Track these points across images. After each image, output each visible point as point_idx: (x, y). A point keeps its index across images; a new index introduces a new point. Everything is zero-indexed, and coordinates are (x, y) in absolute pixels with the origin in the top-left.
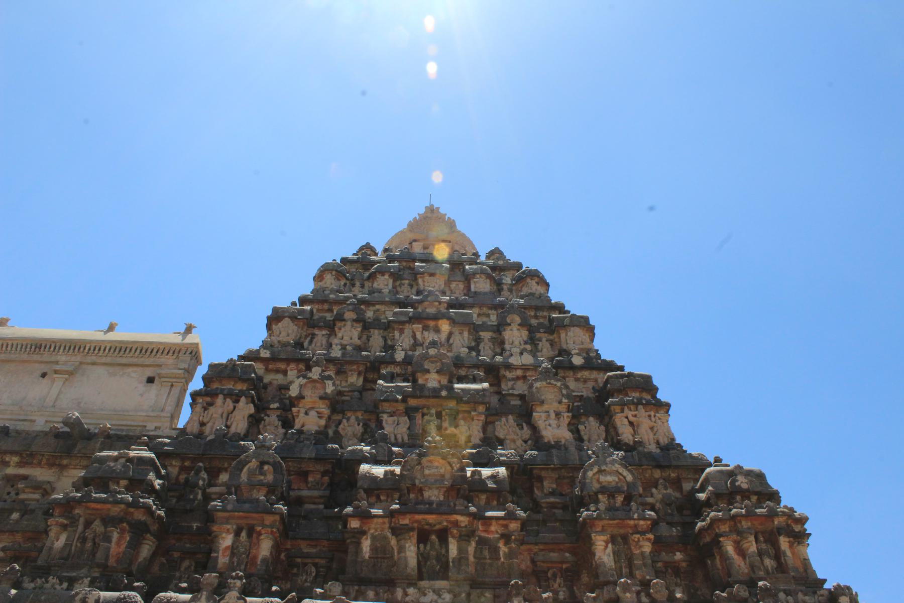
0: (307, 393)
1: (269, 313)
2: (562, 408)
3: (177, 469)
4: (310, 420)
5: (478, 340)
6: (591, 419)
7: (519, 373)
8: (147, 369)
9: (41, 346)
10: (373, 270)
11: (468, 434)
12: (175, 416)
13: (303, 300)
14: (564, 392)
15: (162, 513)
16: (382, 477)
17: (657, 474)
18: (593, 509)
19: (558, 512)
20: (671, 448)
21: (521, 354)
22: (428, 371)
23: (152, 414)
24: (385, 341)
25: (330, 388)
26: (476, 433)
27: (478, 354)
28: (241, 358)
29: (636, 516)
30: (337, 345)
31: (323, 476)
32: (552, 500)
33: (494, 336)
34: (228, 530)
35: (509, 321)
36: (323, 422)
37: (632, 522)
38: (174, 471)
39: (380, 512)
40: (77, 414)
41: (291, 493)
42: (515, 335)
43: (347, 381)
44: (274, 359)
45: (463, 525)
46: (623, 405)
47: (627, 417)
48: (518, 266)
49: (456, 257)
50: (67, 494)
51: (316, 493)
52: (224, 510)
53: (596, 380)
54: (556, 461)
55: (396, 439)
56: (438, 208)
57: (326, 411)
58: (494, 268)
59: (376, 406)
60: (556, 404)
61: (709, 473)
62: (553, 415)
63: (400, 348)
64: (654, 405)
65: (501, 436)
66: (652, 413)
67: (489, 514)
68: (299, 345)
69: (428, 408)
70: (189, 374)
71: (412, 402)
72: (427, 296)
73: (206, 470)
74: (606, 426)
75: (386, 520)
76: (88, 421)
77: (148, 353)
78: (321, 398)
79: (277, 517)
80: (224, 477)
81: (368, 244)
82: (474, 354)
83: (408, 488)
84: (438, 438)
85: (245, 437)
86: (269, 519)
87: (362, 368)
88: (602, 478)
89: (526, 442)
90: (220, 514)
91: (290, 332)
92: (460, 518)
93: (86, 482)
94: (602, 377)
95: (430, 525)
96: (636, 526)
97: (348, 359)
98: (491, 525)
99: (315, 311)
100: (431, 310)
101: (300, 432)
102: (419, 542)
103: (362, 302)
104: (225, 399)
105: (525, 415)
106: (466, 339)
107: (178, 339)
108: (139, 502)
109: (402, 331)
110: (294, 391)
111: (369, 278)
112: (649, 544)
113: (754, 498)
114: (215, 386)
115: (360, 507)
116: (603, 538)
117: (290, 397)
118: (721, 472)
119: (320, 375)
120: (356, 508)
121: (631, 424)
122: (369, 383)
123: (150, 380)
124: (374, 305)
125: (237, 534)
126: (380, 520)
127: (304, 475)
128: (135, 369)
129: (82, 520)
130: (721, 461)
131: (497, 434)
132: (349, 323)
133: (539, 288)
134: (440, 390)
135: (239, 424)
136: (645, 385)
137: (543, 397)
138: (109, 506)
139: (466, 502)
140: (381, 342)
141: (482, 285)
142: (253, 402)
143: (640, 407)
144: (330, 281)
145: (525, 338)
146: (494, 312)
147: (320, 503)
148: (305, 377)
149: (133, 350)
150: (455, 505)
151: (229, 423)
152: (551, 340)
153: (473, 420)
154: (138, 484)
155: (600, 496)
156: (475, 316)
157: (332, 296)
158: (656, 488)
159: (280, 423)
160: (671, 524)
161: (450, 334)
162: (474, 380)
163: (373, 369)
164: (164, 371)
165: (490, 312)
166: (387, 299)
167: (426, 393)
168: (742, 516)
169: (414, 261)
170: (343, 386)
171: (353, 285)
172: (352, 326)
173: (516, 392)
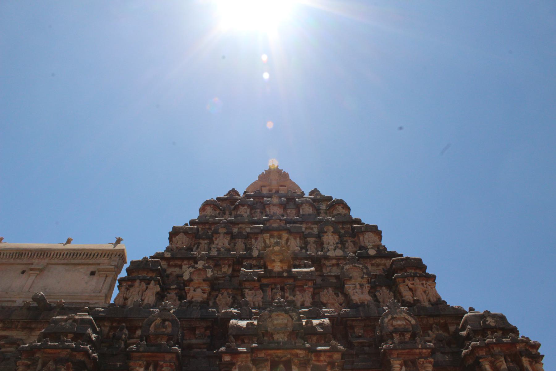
0: (195, 278)
1: (171, 230)
2: (364, 282)
3: (108, 328)
4: (197, 294)
5: (306, 243)
6: (384, 288)
7: (334, 262)
8: (90, 266)
9: (22, 253)
10: (237, 203)
11: (302, 300)
12: (108, 295)
13: (192, 222)
14: (365, 271)
15: (96, 355)
16: (245, 327)
17: (431, 321)
18: (390, 343)
19: (366, 349)
20: (439, 303)
21: (335, 250)
22: (274, 261)
23: (92, 295)
24: (246, 246)
25: (210, 273)
26: (307, 299)
27: (307, 250)
28: (151, 257)
29: (420, 346)
30: (214, 248)
31: (206, 330)
32: (361, 340)
33: (316, 240)
34: (140, 365)
35: (325, 230)
36: (205, 296)
37: (417, 351)
38: (106, 330)
39: (244, 349)
40: (42, 293)
41: (185, 342)
42: (330, 239)
43: (221, 271)
44: (172, 258)
45: (301, 356)
46: (404, 278)
47: (407, 285)
48: (330, 198)
49: (289, 194)
50: (31, 343)
51: (200, 341)
52: (137, 351)
53: (385, 265)
54: (362, 315)
55: (254, 305)
57: (206, 288)
58: (314, 200)
59: (240, 284)
60: (360, 279)
61: (467, 317)
62: (358, 286)
63: (255, 249)
64: (425, 277)
65: (325, 301)
66: (424, 282)
67: (319, 348)
68: (190, 249)
69: (275, 285)
70: (118, 269)
71: (265, 281)
72: (272, 216)
73: (127, 328)
74: (394, 293)
75: (249, 355)
76: (51, 300)
77: (92, 256)
78: (204, 280)
79: (174, 356)
80: (139, 333)
81: (233, 189)
82: (304, 251)
83: (262, 333)
84: (282, 300)
85: (154, 307)
86: (168, 357)
87: (230, 262)
88: (395, 323)
89: (341, 304)
90: (135, 354)
91: (184, 241)
92: (299, 352)
93: (45, 335)
94: (388, 262)
95: (279, 357)
96: (420, 353)
97: (222, 256)
98: (320, 356)
99: (200, 229)
100: (275, 225)
101: (190, 302)
103: (231, 222)
104: (141, 282)
105: (339, 286)
106: (298, 243)
107: (111, 247)
109: (256, 239)
110: (186, 277)
111: (234, 209)
112: (431, 365)
113: (500, 333)
114: (134, 275)
115: (230, 347)
116: (398, 362)
117: (184, 280)
118: (475, 316)
119: (203, 266)
120: (228, 347)
121: (411, 289)
122: (236, 271)
123: (93, 273)
124: (238, 224)
126: (245, 355)
127: (193, 330)
128: (83, 266)
129: (40, 361)
130: (474, 310)
131: (321, 300)
132: (222, 235)
133: (344, 210)
134: (283, 272)
135: (150, 297)
136: (417, 265)
137: (351, 275)
138: (60, 351)
139: (302, 341)
140: (243, 246)
141: (307, 210)
142: (159, 284)
143: (416, 278)
144: (209, 211)
145: (337, 241)
147: (204, 348)
148: (193, 267)
149: (82, 255)
150: (295, 343)
151: (143, 298)
152: (354, 242)
153: (305, 291)
154: (80, 336)
155: (394, 335)
156: (304, 229)
157: (211, 220)
158: (432, 331)
159: (177, 298)
160: (444, 353)
161: (287, 240)
162: (305, 267)
163: (238, 262)
164: (102, 267)
165: (313, 226)
166: (246, 220)
167: (274, 275)
168: (494, 344)
169: (264, 197)
170: (219, 274)
171: (225, 214)
172: (224, 237)
173: (333, 274)
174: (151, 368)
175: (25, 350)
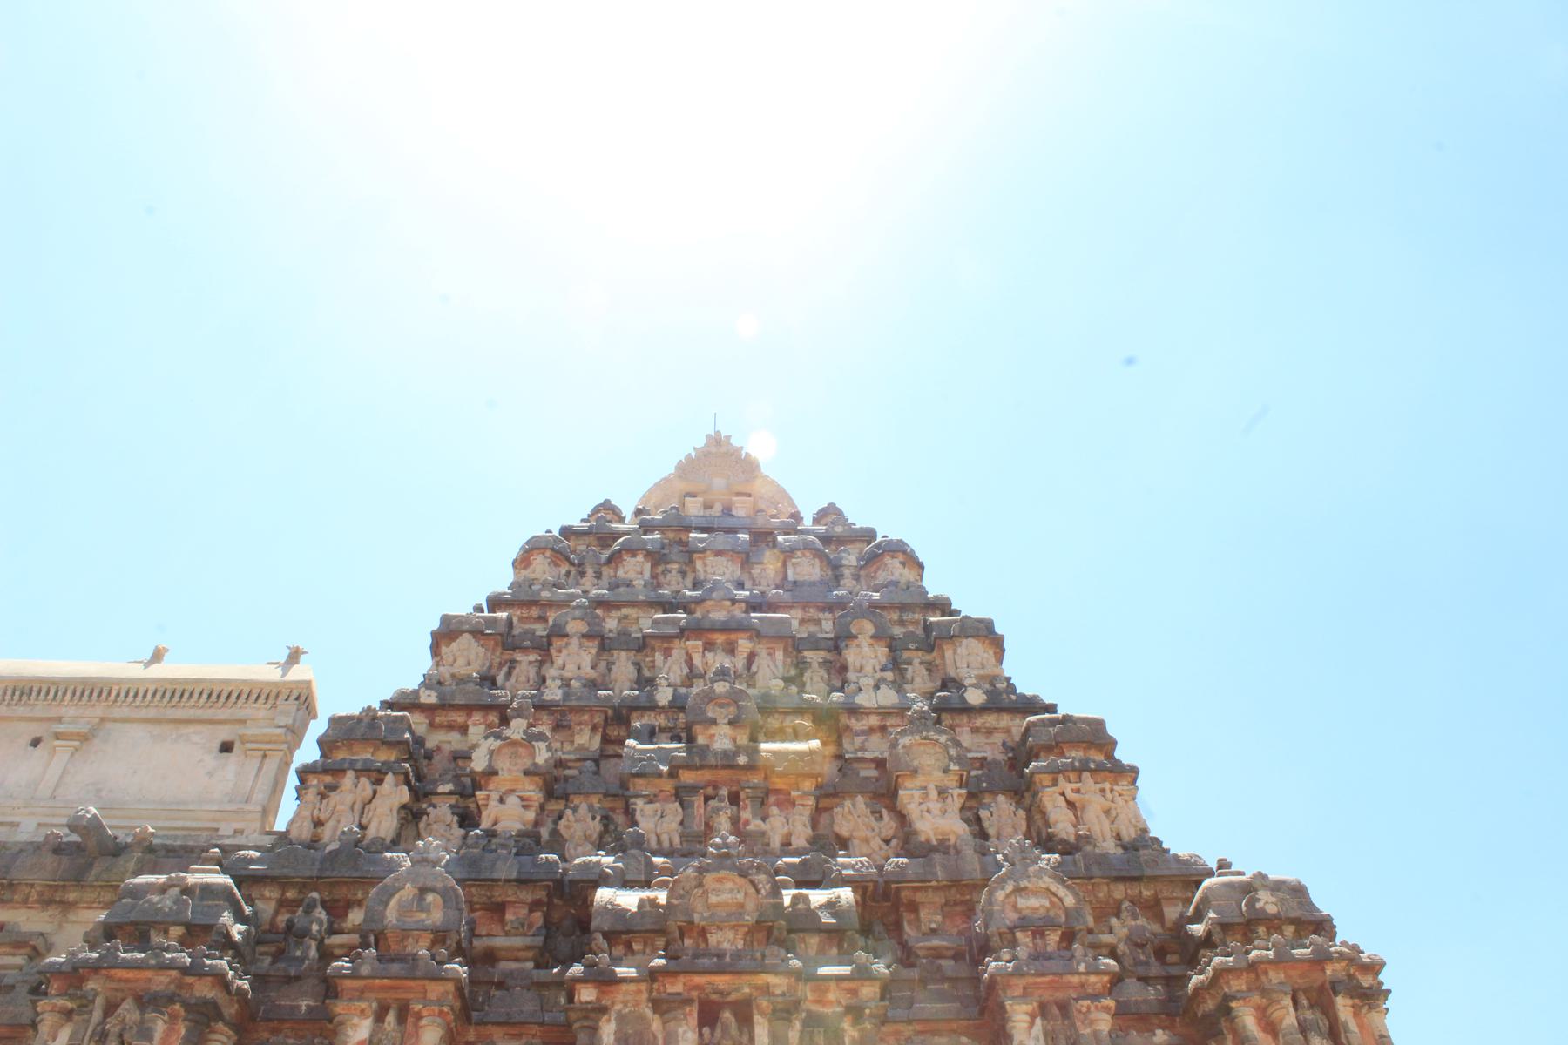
0: (503, 764)
1: (436, 625)
2: (951, 781)
3: (273, 904)
4: (507, 813)
5: (802, 665)
6: (1001, 798)
7: (874, 721)
8: (220, 727)
9: (31, 690)
10: (616, 547)
11: (785, 830)
12: (269, 810)
13: (495, 602)
14: (953, 752)
15: (245, 984)
16: (634, 909)
17: (1119, 891)
18: (1007, 957)
19: (947, 964)
20: (1141, 845)
21: (877, 687)
22: (714, 722)
23: (228, 807)
24: (639, 670)
25: (542, 755)
26: (800, 828)
27: (802, 689)
28: (388, 705)
29: (1082, 968)
30: (554, 679)
31: (531, 911)
32: (935, 943)
33: (829, 656)
34: (362, 1011)
35: (854, 631)
36: (531, 815)
37: (1075, 979)
38: (267, 908)
39: (630, 972)
40: (94, 811)
41: (476, 943)
42: (865, 655)
43: (572, 742)
44: (444, 706)
45: (778, 991)
46: (1055, 772)
47: (1063, 794)
48: (869, 535)
49: (760, 522)
50: (73, 954)
51: (518, 942)
52: (355, 975)
53: (1008, 731)
54: (940, 874)
55: (659, 841)
56: (728, 438)
57: (536, 796)
58: (826, 539)
59: (624, 785)
60: (938, 774)
61: (1209, 888)
62: (934, 794)
63: (665, 683)
64: (1111, 771)
65: (845, 833)
66: (1107, 786)
67: (824, 971)
68: (488, 680)
69: (716, 787)
70: (295, 735)
71: (687, 777)
72: (711, 590)
73: (324, 904)
74: (1028, 811)
75: (643, 986)
76: (114, 822)
77: (223, 699)
78: (527, 773)
79: (450, 986)
80: (356, 917)
82: (794, 689)
83: (680, 928)
84: (732, 839)
85: (394, 844)
86: (435, 990)
87: (599, 719)
88: (1022, 902)
89: (887, 842)
90: (348, 983)
91: (472, 657)
92: (772, 979)
93: (109, 932)
94: (1018, 725)
95: (721, 993)
96: (1082, 985)
97: (574, 703)
98: (827, 990)
99: (515, 620)
100: (719, 616)
101: (491, 834)
102: (701, 1025)
103: (600, 603)
104: (357, 778)
105: (885, 795)
106: (780, 664)
107: (275, 675)
108: (205, 965)
109: (667, 653)
110: (479, 763)
111: (609, 561)
112: (1107, 1017)
113: (1289, 930)
114: (341, 755)
115: (595, 964)
116: (1026, 1008)
117: (472, 772)
118: (1230, 885)
119: (525, 732)
120: (590, 966)
121: (1071, 805)
122: (612, 744)
123: (226, 748)
124: (618, 608)
125: (380, 1017)
126: (632, 987)
127: (498, 909)
128: (199, 728)
129: (99, 1001)
130: (1229, 865)
131: (836, 828)
132: (575, 641)
133: (906, 571)
134: (736, 754)
135: (383, 822)
136: (1094, 736)
137: (916, 763)
138: (149, 974)
139: (782, 952)
140: (631, 672)
141: (807, 570)
142: (407, 783)
143: (1086, 775)
144: (541, 568)
145: (884, 660)
146: (828, 615)
147: (526, 960)
148: (498, 736)
149: (196, 695)
150: (763, 956)
151: (364, 821)
152: (930, 663)
153: (794, 805)
154: (199, 933)
155: (1019, 934)
156: (795, 623)
157: (545, 594)
158: (1118, 917)
159: (456, 818)
160: (1145, 980)
161: (751, 657)
162: (797, 736)
163: (618, 719)
164: (250, 731)
165: (821, 616)
166: (641, 598)
167: (712, 761)
168: (1270, 962)
169: (688, 529)
170: (567, 752)
171: (583, 574)
172: (581, 645)
173: (868, 755)
174: (391, 1018)
175: (56, 972)
